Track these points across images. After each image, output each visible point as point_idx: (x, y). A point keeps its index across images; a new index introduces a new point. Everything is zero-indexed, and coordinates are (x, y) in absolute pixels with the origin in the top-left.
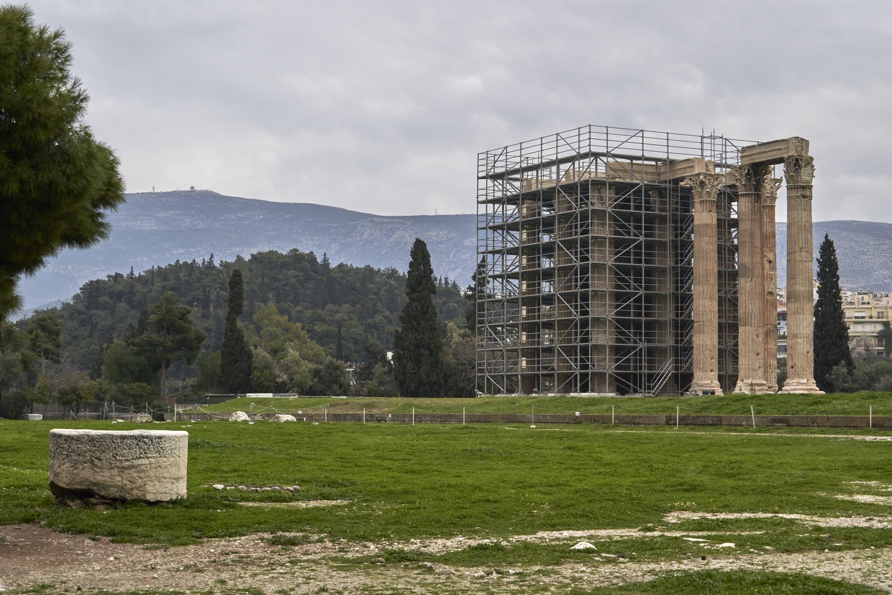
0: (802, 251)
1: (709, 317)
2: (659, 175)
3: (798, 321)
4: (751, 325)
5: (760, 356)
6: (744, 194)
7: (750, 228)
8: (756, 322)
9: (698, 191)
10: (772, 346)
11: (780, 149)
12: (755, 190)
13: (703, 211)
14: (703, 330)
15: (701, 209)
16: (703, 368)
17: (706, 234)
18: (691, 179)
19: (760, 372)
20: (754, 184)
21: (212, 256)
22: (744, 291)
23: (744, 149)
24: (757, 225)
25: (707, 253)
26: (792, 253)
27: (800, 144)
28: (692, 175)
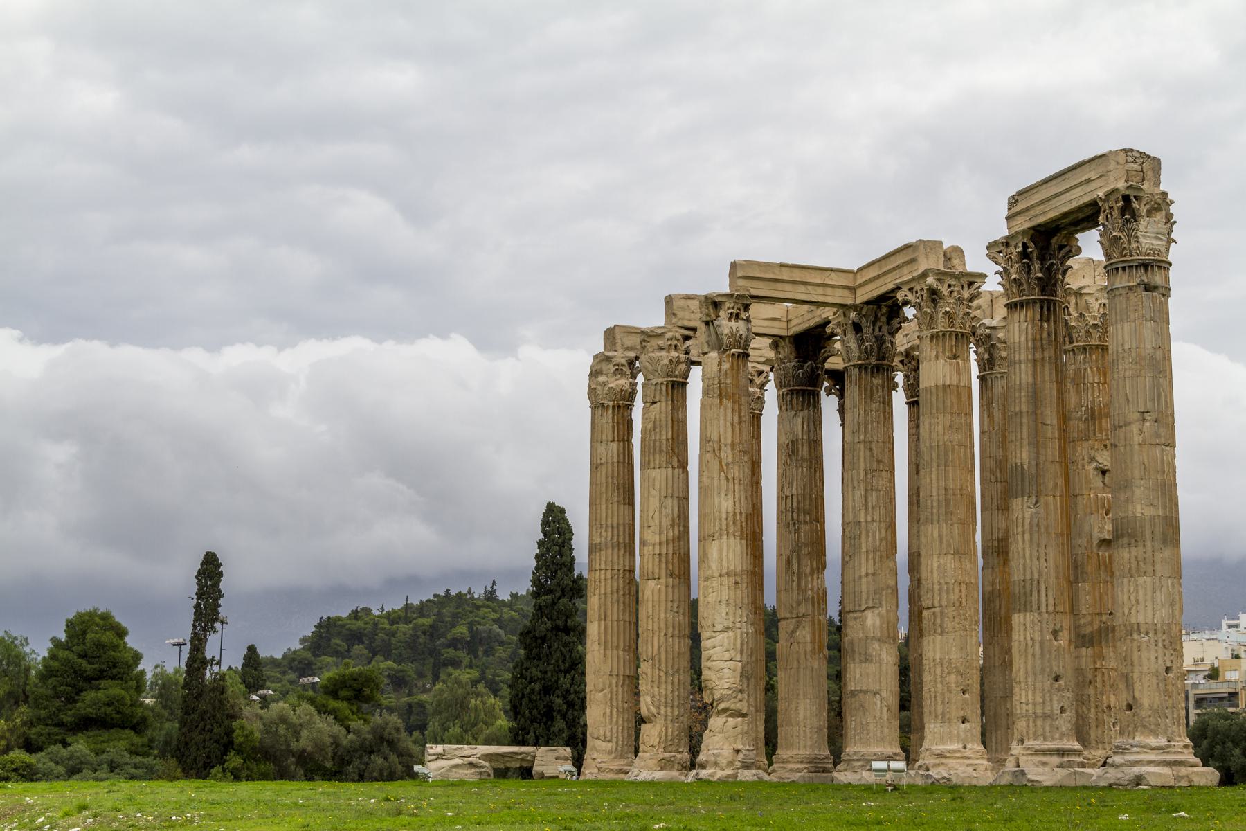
0: (1144, 420)
1: (957, 596)
2: (853, 290)
3: (1141, 592)
4: (1039, 608)
5: (1062, 682)
6: (1015, 304)
7: (1030, 380)
8: (1051, 602)
9: (926, 312)
10: (1113, 664)
11: (1089, 181)
12: (1043, 291)
13: (937, 357)
14: (941, 627)
15: (934, 354)
16: (943, 714)
17: (945, 407)
18: (911, 290)
19: (1065, 722)
20: (1038, 278)
21: (494, 583)
22: (1020, 529)
23: (1013, 202)
24: (1047, 373)
25: (946, 452)
26: (1120, 427)
27: (1136, 166)
28: (913, 279)
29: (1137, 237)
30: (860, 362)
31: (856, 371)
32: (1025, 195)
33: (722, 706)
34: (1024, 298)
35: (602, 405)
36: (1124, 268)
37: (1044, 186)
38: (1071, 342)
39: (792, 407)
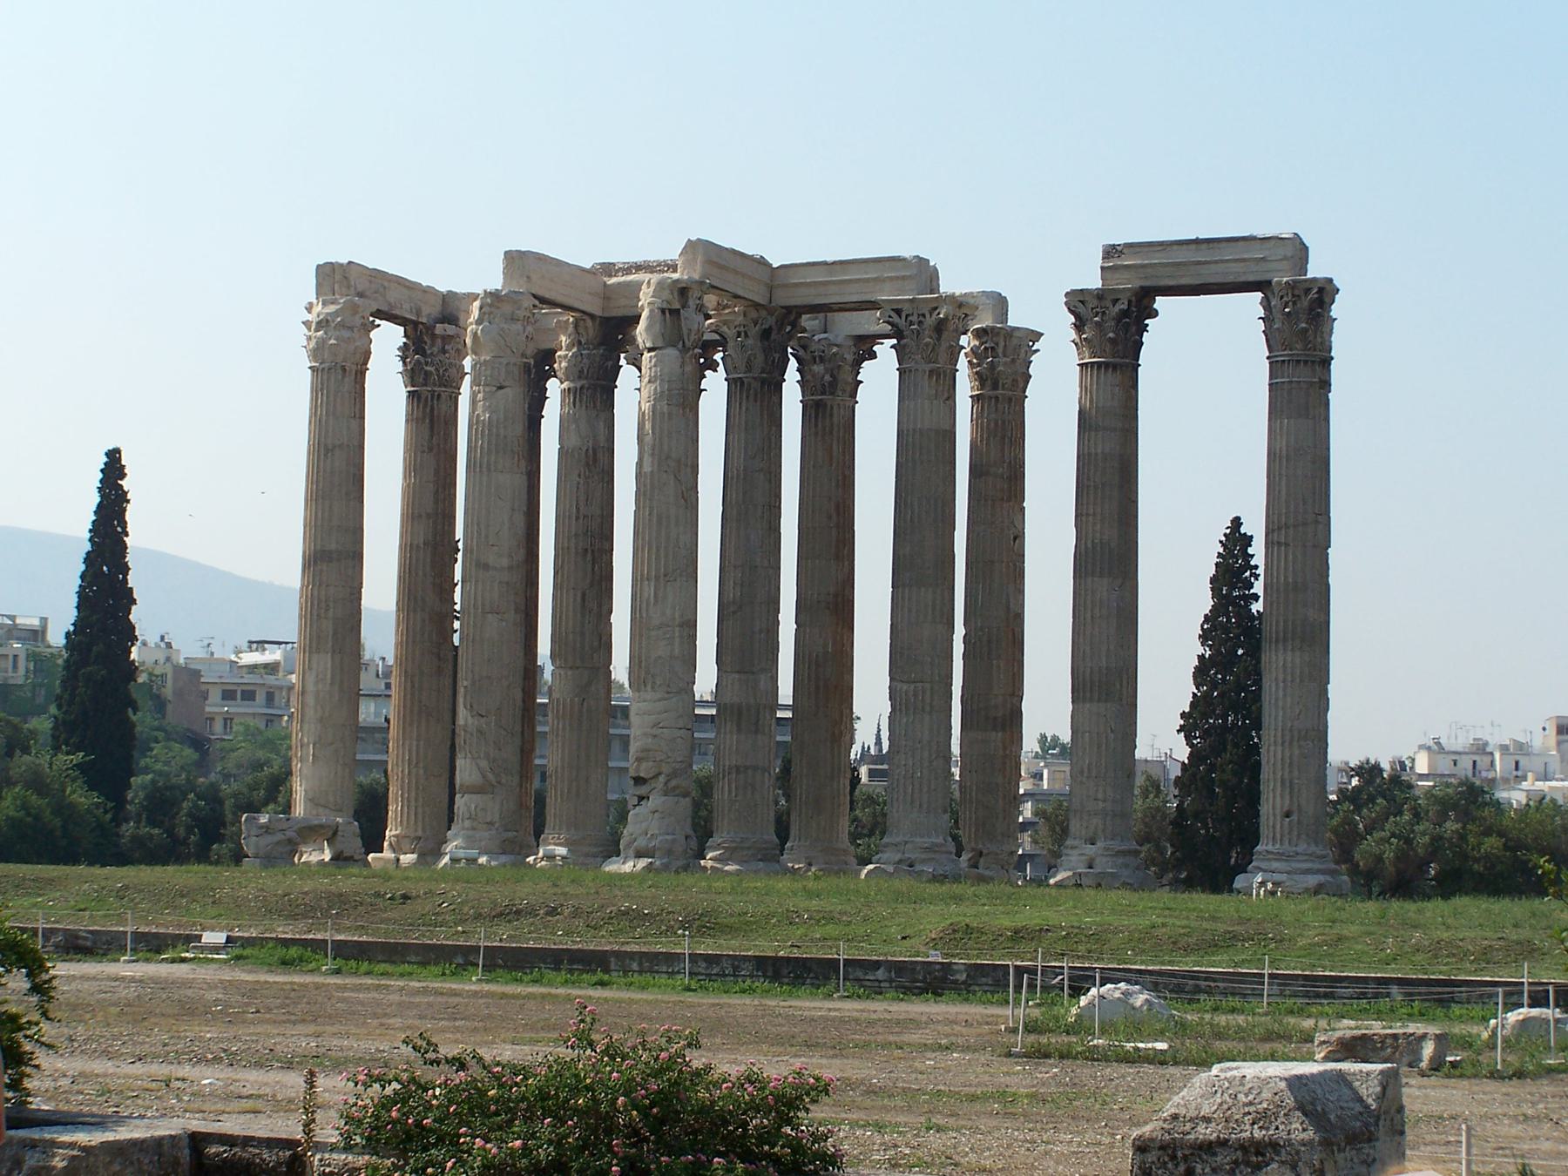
2: (771, 289)
6: (1107, 365)
9: (927, 345)
18: (898, 312)
23: (1111, 252)
29: (1323, 333)
30: (765, 375)
31: (757, 385)
32: (1138, 249)
33: (673, 783)
34: (1118, 360)
35: (344, 369)
36: (1306, 362)
37: (1175, 247)
38: (995, 387)
39: (595, 407)
